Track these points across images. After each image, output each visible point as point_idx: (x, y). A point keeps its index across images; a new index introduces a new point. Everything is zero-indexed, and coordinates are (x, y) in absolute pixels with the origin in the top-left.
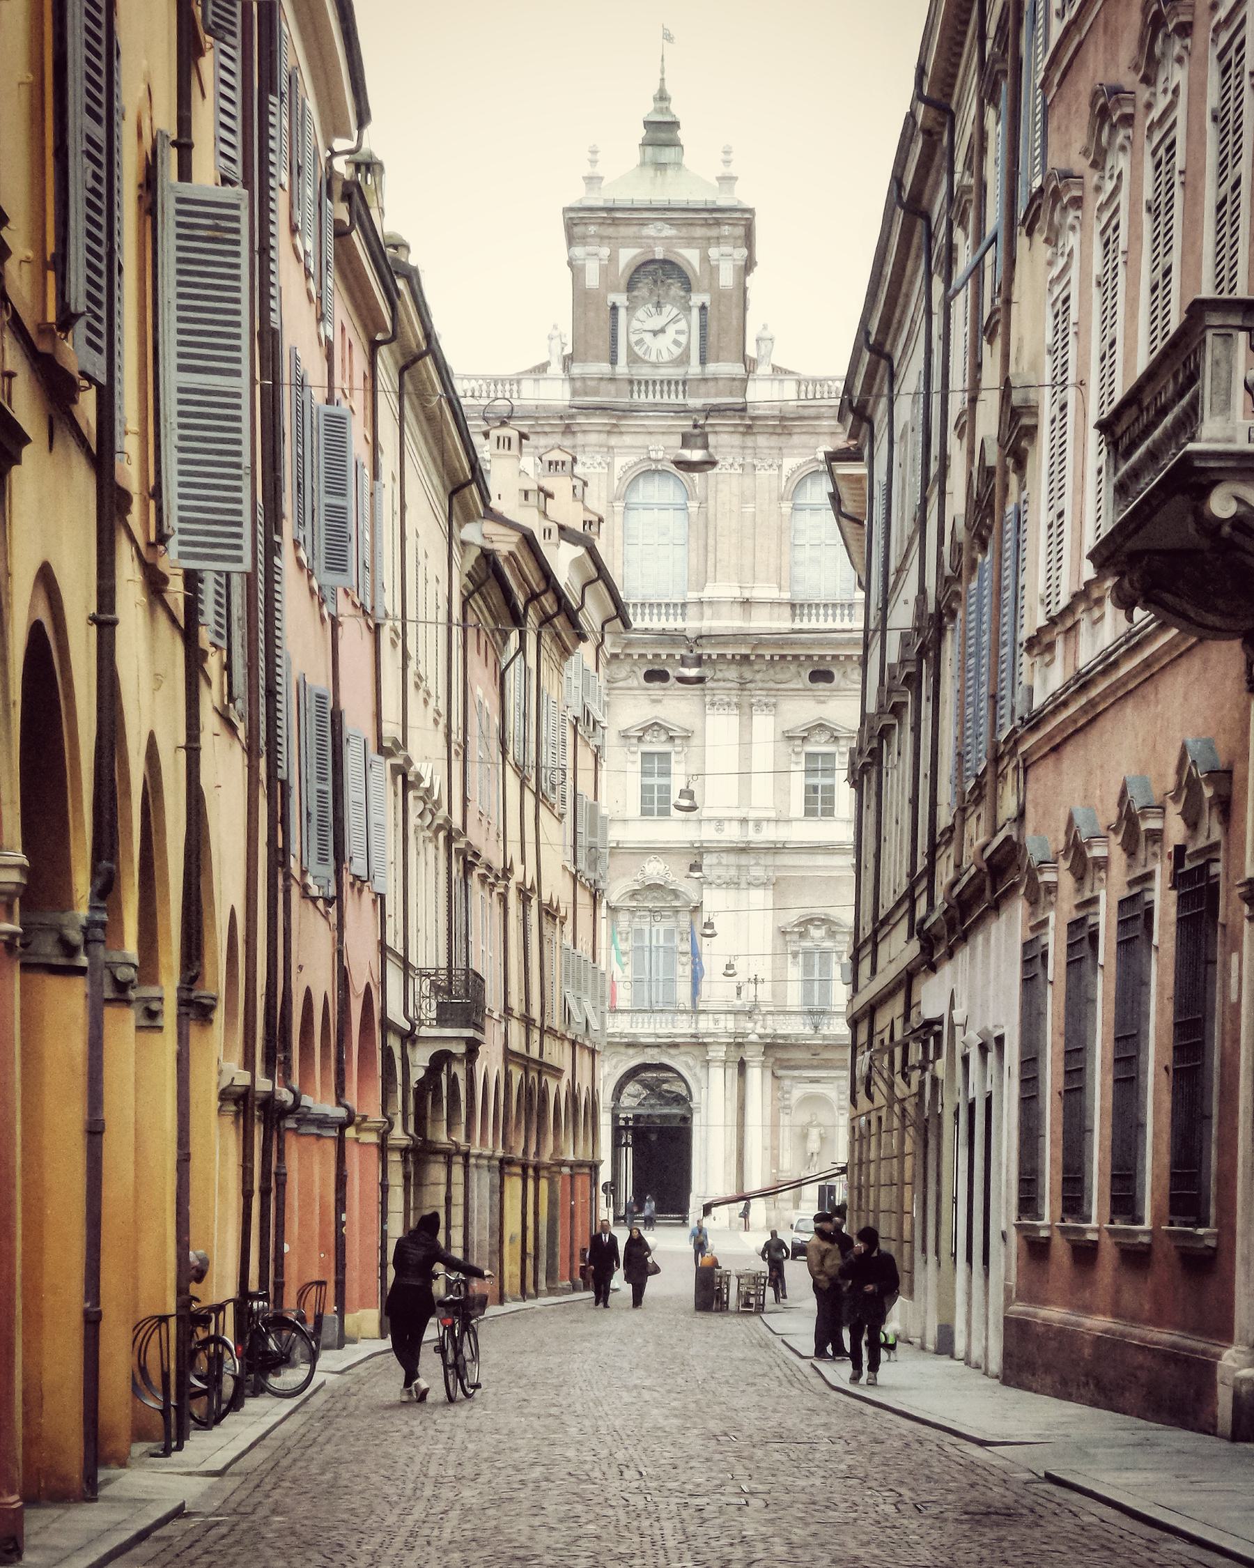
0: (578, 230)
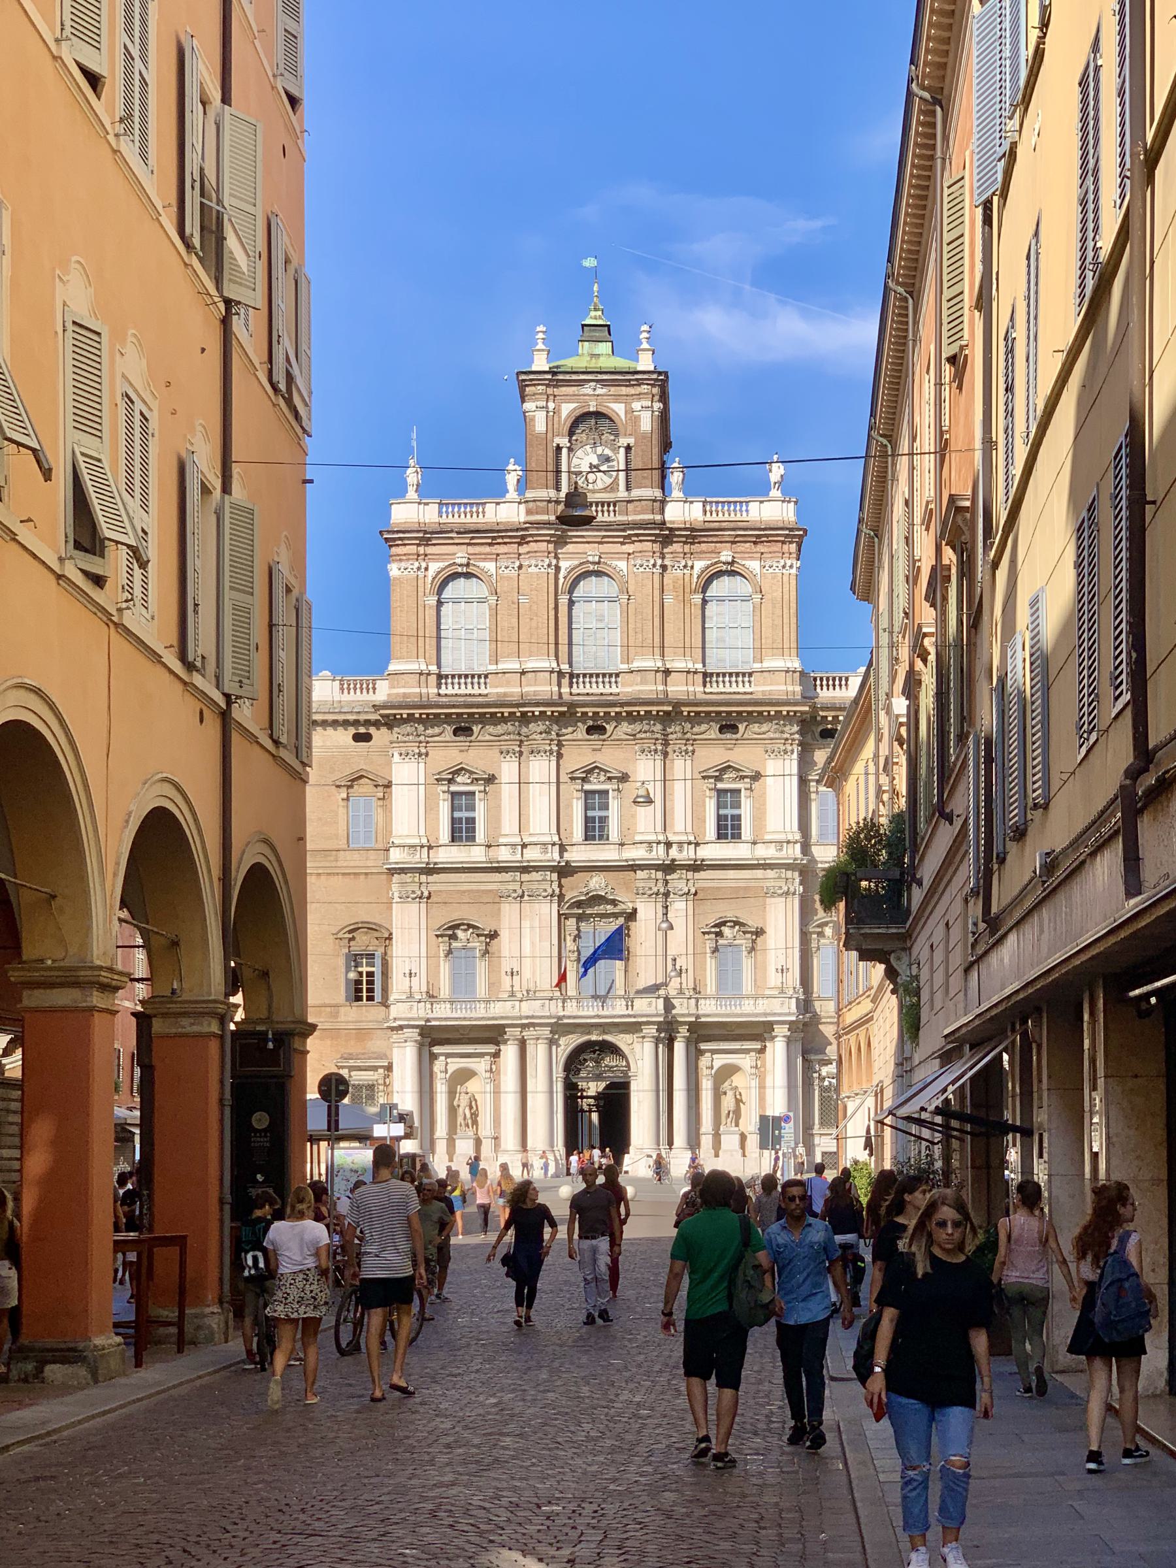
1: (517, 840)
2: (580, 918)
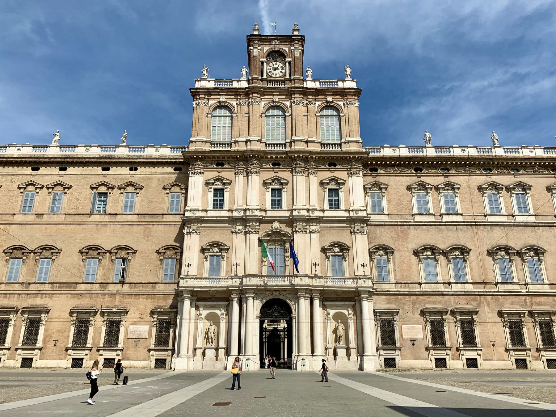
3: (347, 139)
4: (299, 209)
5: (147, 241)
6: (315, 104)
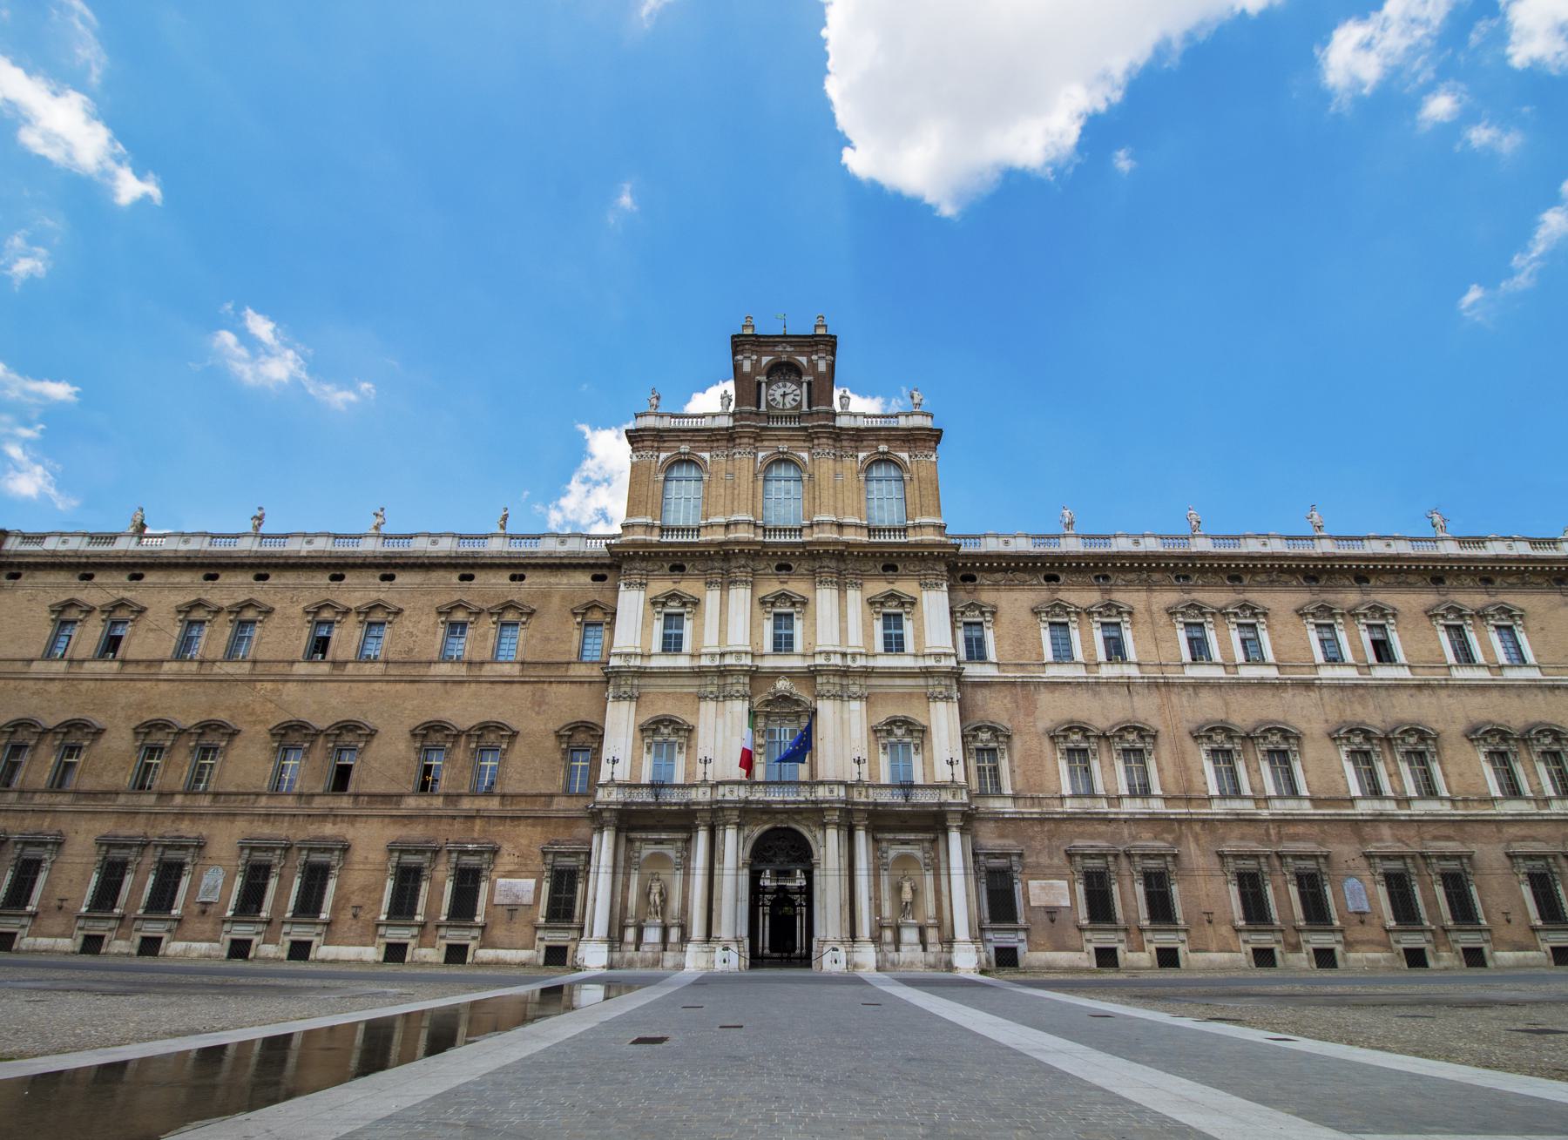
0: (740, 348)
1: (717, 650)
2: (768, 715)
3: (917, 521)
4: (828, 654)
5: (538, 713)
6: (857, 457)
